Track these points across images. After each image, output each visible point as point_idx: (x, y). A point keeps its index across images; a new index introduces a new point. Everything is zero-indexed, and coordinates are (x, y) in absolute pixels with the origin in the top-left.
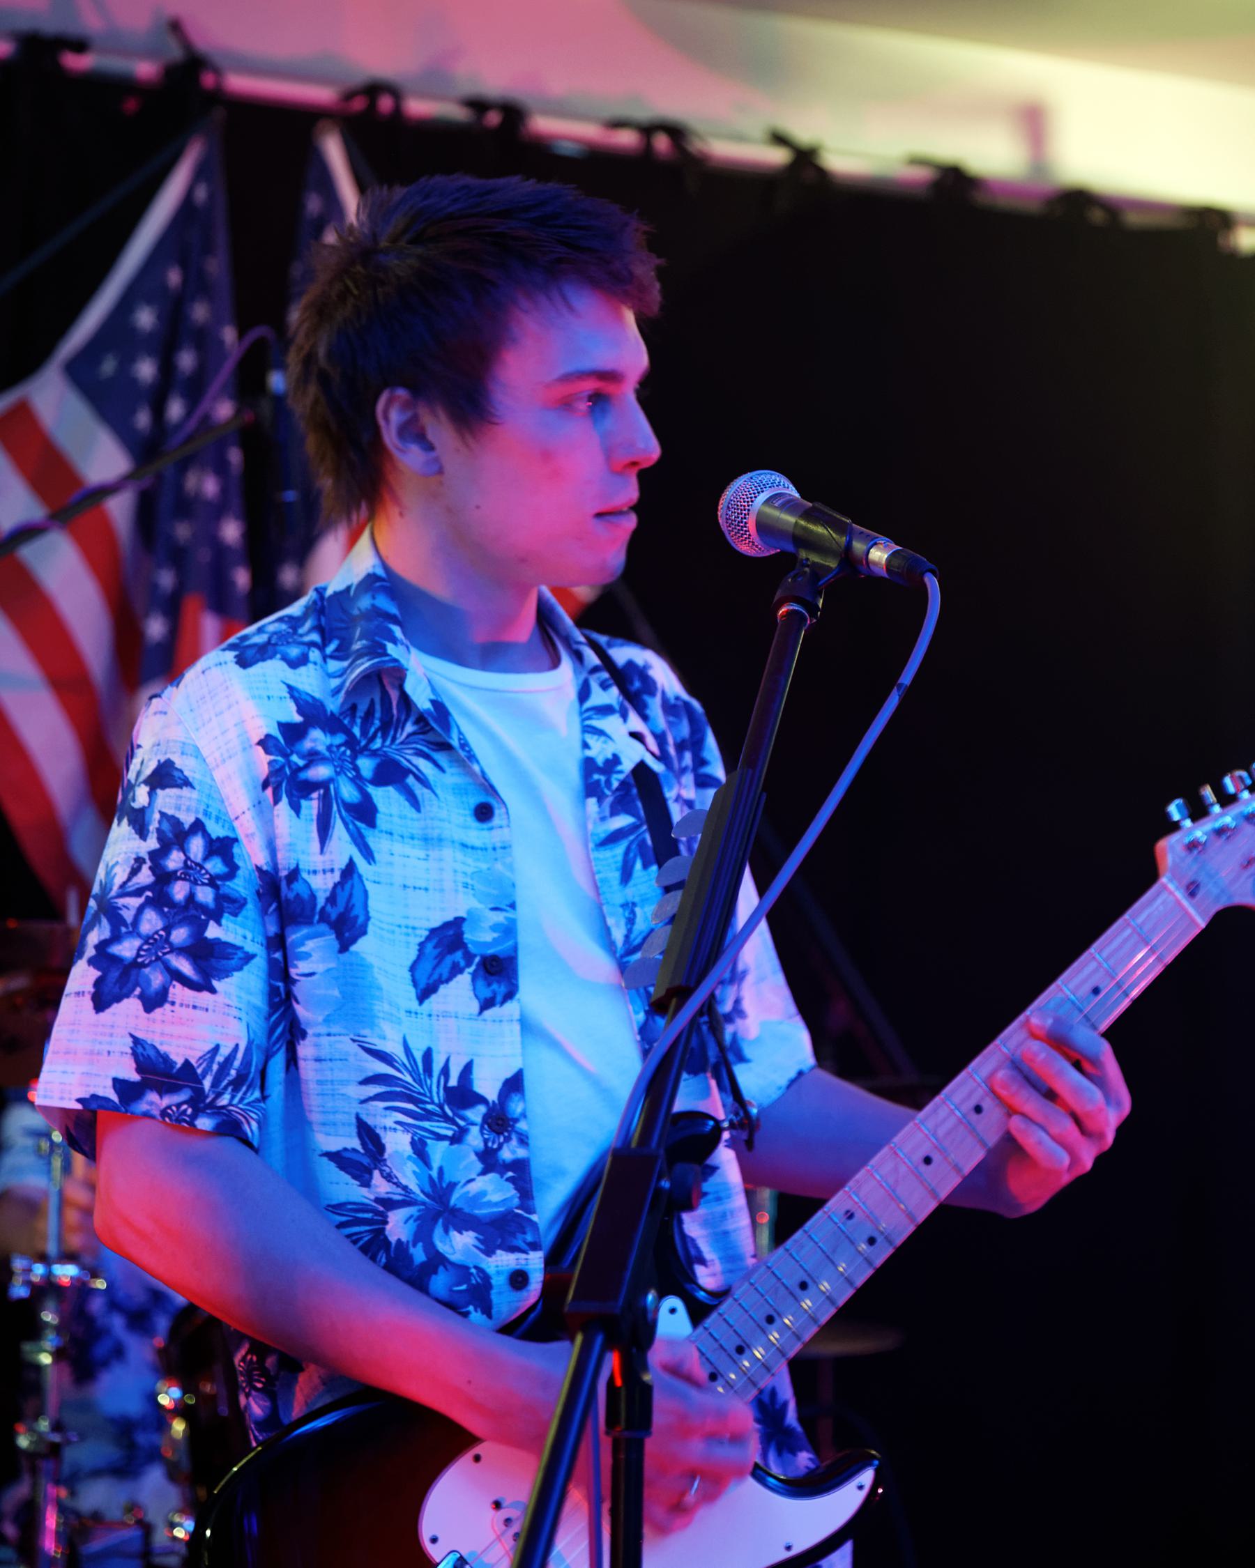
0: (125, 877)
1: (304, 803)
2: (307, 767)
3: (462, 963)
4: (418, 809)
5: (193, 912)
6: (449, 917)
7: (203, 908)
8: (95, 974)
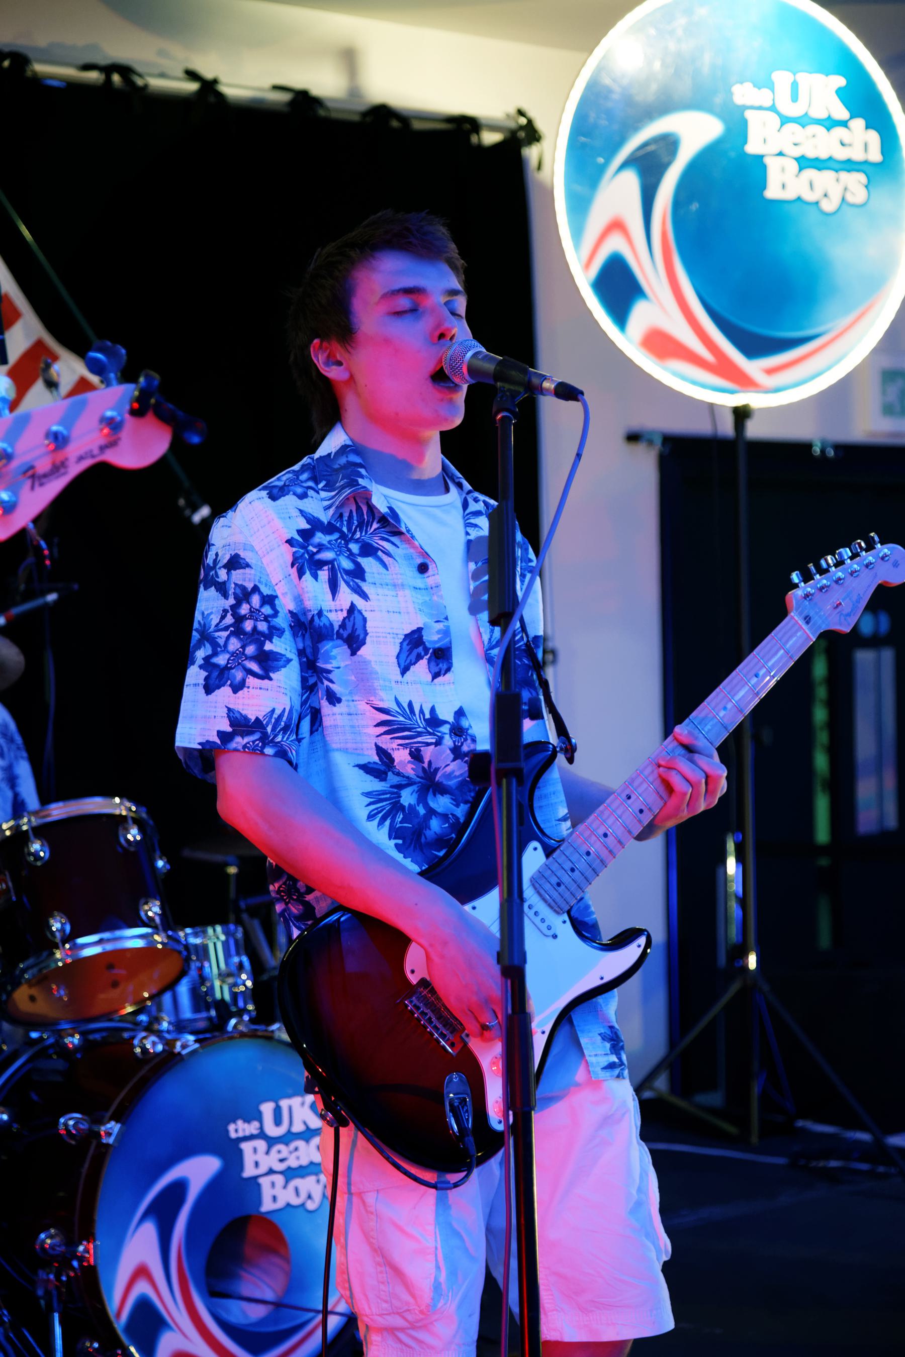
0: (218, 621)
1: (319, 572)
2: (318, 552)
3: (423, 654)
4: (387, 570)
5: (256, 636)
6: (415, 628)
7: (262, 634)
8: (204, 674)
